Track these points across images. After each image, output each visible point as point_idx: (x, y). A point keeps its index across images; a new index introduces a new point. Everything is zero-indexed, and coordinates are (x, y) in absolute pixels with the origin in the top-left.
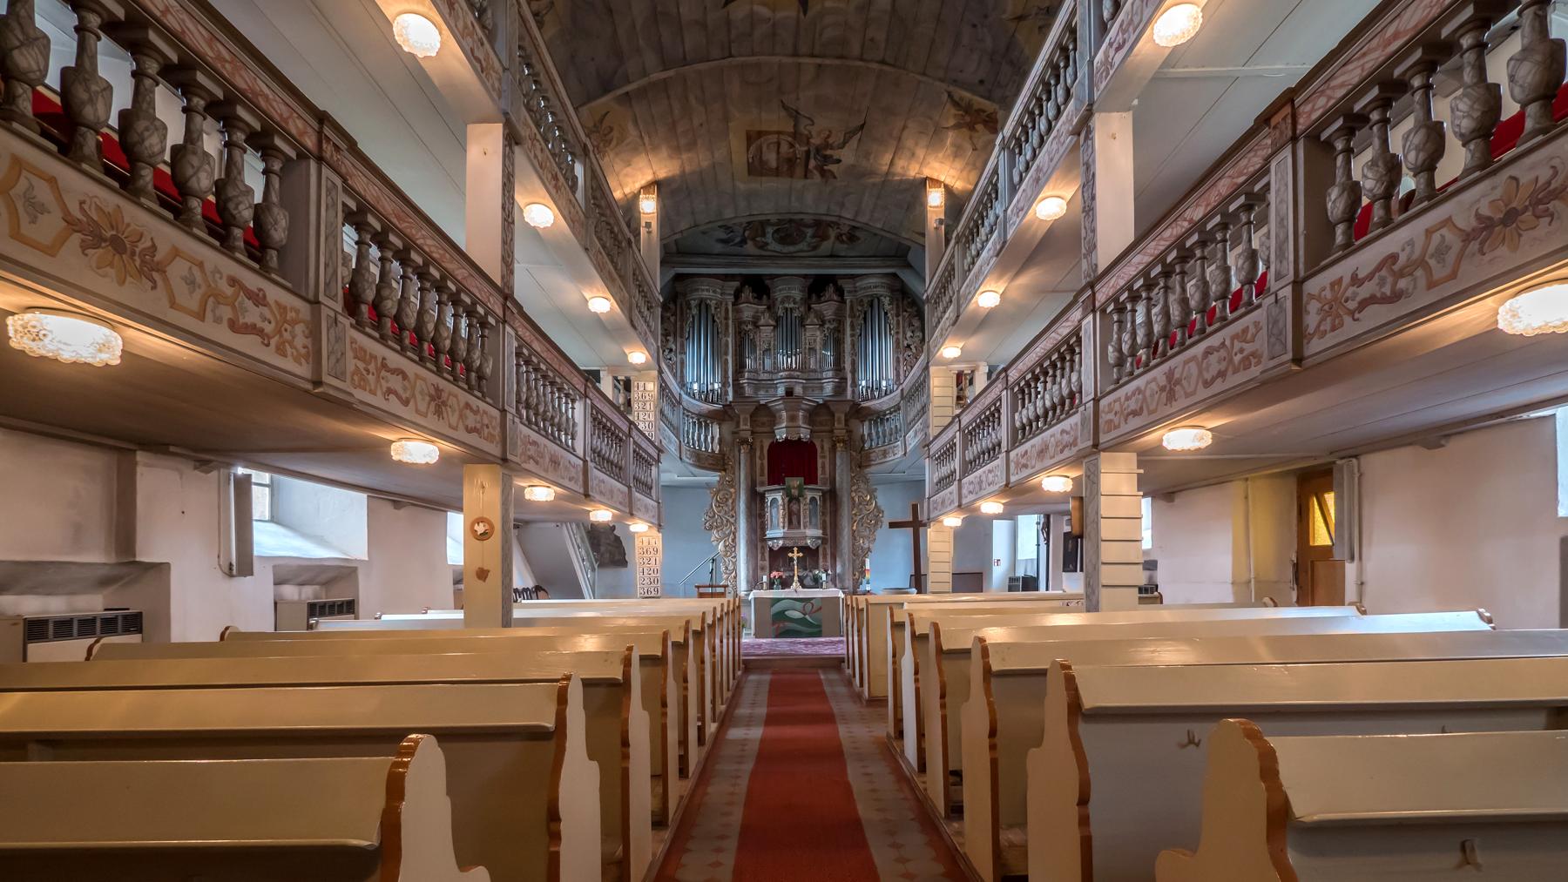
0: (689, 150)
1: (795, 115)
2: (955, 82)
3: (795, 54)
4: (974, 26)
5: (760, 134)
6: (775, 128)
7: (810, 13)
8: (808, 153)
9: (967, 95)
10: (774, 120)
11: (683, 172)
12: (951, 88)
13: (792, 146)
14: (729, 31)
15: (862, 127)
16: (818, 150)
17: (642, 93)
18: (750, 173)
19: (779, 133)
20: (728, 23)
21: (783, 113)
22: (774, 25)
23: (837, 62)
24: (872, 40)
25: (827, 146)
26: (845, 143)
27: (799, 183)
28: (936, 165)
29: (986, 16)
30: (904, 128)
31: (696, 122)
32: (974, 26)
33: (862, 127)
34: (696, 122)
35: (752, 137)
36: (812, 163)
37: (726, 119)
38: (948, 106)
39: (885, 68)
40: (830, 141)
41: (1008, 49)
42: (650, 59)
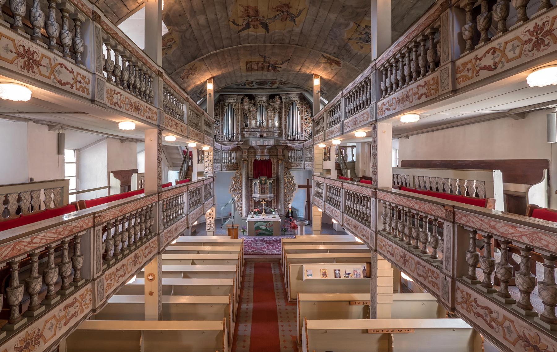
3: (264, 43)
7: (270, 33)
14: (240, 39)
20: (239, 37)
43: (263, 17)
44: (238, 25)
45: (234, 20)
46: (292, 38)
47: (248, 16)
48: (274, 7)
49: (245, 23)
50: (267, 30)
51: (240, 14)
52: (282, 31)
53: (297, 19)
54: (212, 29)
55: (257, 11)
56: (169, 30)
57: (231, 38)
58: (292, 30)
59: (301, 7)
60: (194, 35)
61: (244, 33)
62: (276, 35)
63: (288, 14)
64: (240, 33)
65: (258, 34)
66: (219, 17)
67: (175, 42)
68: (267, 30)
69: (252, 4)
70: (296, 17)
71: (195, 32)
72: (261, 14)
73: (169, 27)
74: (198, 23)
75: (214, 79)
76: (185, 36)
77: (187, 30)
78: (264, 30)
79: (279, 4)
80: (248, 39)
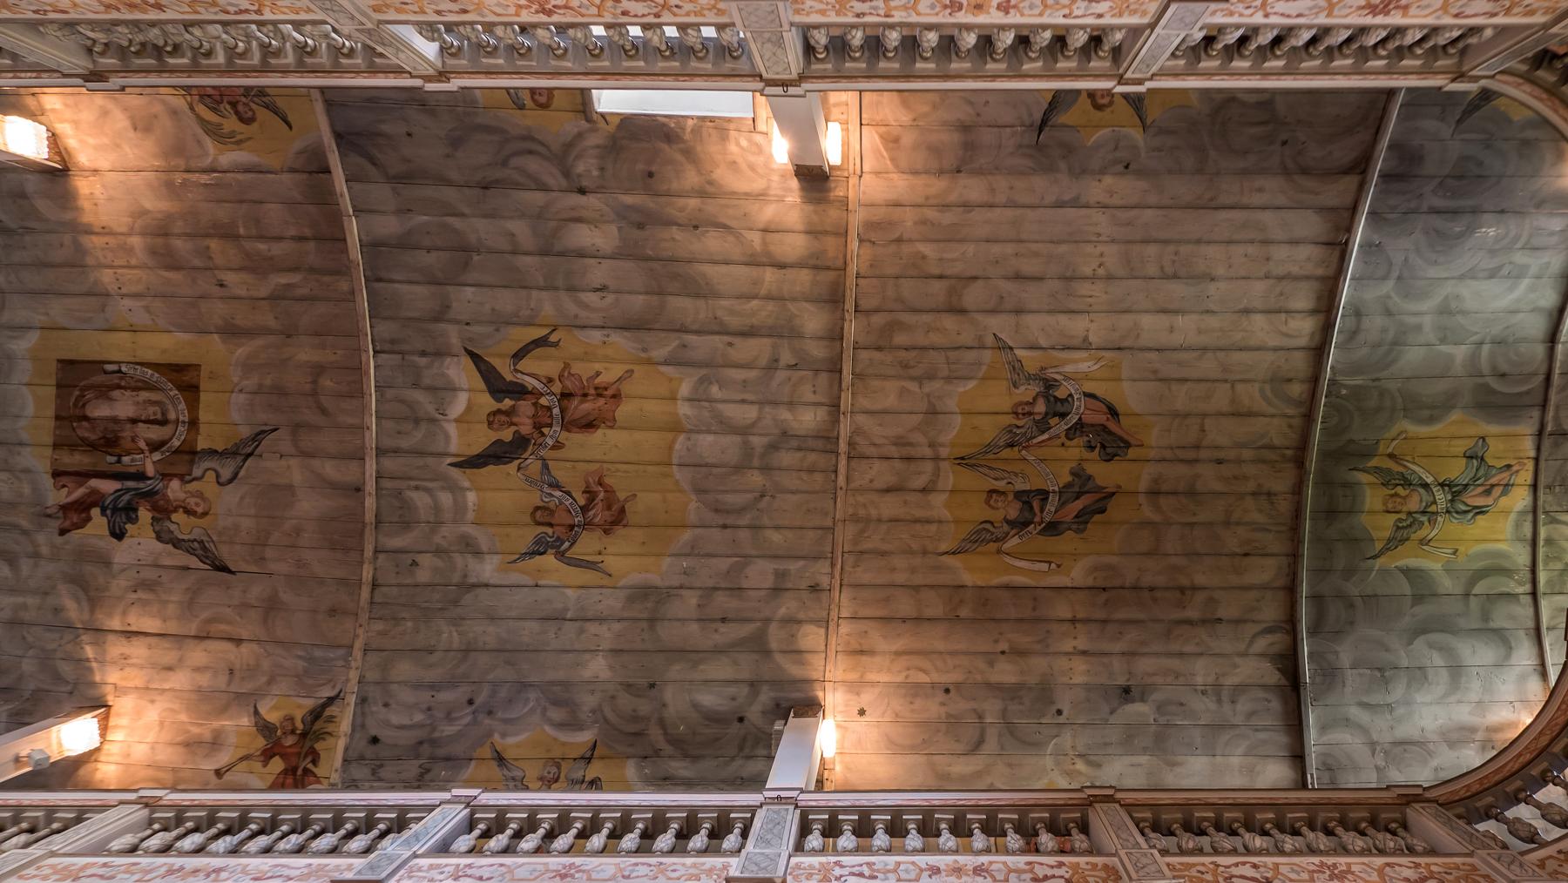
0: (153, 252)
1: (243, 451)
2: (363, 701)
3: (381, 452)
4: (471, 702)
5: (191, 391)
6: (203, 416)
8: (141, 476)
9: (345, 725)
10: (223, 415)
11: (89, 231)
12: (352, 699)
13: (155, 446)
14: (423, 354)
15: (224, 569)
16: (149, 495)
17: (323, 197)
18: (67, 364)
19: (193, 423)
20: (440, 354)
21: (245, 432)
22: (433, 421)
23: (370, 517)
24: (414, 563)
25: (162, 511)
26: (177, 543)
27: (38, 461)
28: (153, 714)
29: (490, 713)
30: (238, 641)
31: (230, 278)
32: (471, 702)
33: (224, 569)
34: (230, 278)
35: (183, 377)
36: (108, 487)
37: (231, 332)
38: (309, 703)
39: (365, 593)
40: (178, 517)
41: (448, 759)
42: (388, 226)
43: (558, 446)
44: (518, 356)
45: (556, 345)
46: (426, 560)
47: (566, 396)
48: (607, 480)
49: (531, 382)
50: (473, 462)
51: (577, 368)
52: (470, 516)
53: (549, 560)
54: (528, 259)
55: (589, 425)
56: (603, 115)
57: (437, 319)
58: (478, 553)
59: (611, 562)
60: (518, 186)
61: (461, 372)
62: (446, 499)
63: (572, 527)
64: (467, 361)
65: (452, 429)
66: (591, 298)
67: (522, 107)
68: (473, 462)
69: (624, 410)
70: (561, 556)
71: (538, 198)
72: (574, 439)
73: (617, 121)
74: (579, 220)
75: (56, 174)
76: (531, 152)
77: (567, 174)
78: (476, 450)
79: (622, 496)
80: (416, 385)
